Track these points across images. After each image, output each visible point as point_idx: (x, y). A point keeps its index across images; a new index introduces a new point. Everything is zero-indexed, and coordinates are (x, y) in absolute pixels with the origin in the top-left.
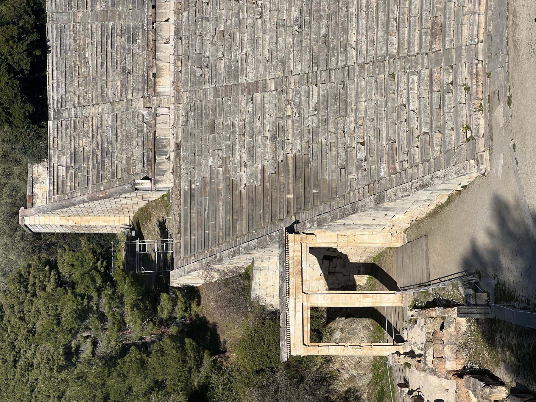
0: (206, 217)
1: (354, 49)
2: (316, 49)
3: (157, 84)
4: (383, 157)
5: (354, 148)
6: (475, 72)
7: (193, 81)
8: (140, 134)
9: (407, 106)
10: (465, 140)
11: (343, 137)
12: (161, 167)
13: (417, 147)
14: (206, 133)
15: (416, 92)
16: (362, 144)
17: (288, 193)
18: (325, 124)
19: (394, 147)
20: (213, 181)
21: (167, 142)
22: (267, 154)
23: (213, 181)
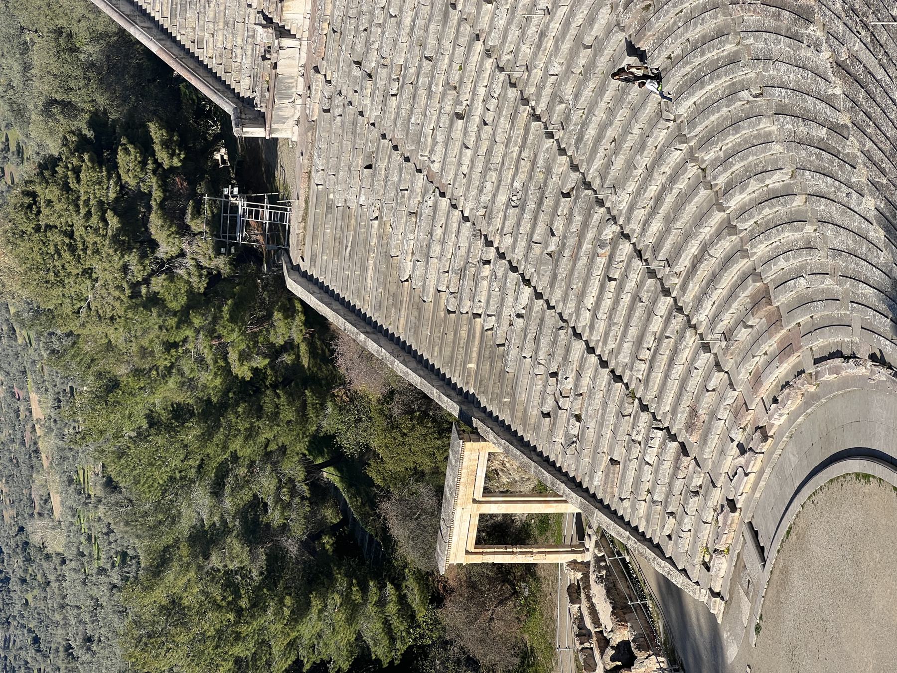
0: (347, 254)
1: (589, 310)
2: (537, 249)
3: (284, 9)
4: (601, 464)
5: (567, 410)
6: (729, 522)
7: (345, 72)
8: (250, 40)
9: (642, 446)
10: (701, 559)
11: (555, 384)
12: (280, 113)
13: (645, 501)
14: (359, 156)
15: (657, 446)
16: (578, 418)
17: (470, 362)
18: (533, 341)
19: (617, 470)
20: (363, 223)
21: (292, 83)
22: (446, 279)
23: (363, 223)
